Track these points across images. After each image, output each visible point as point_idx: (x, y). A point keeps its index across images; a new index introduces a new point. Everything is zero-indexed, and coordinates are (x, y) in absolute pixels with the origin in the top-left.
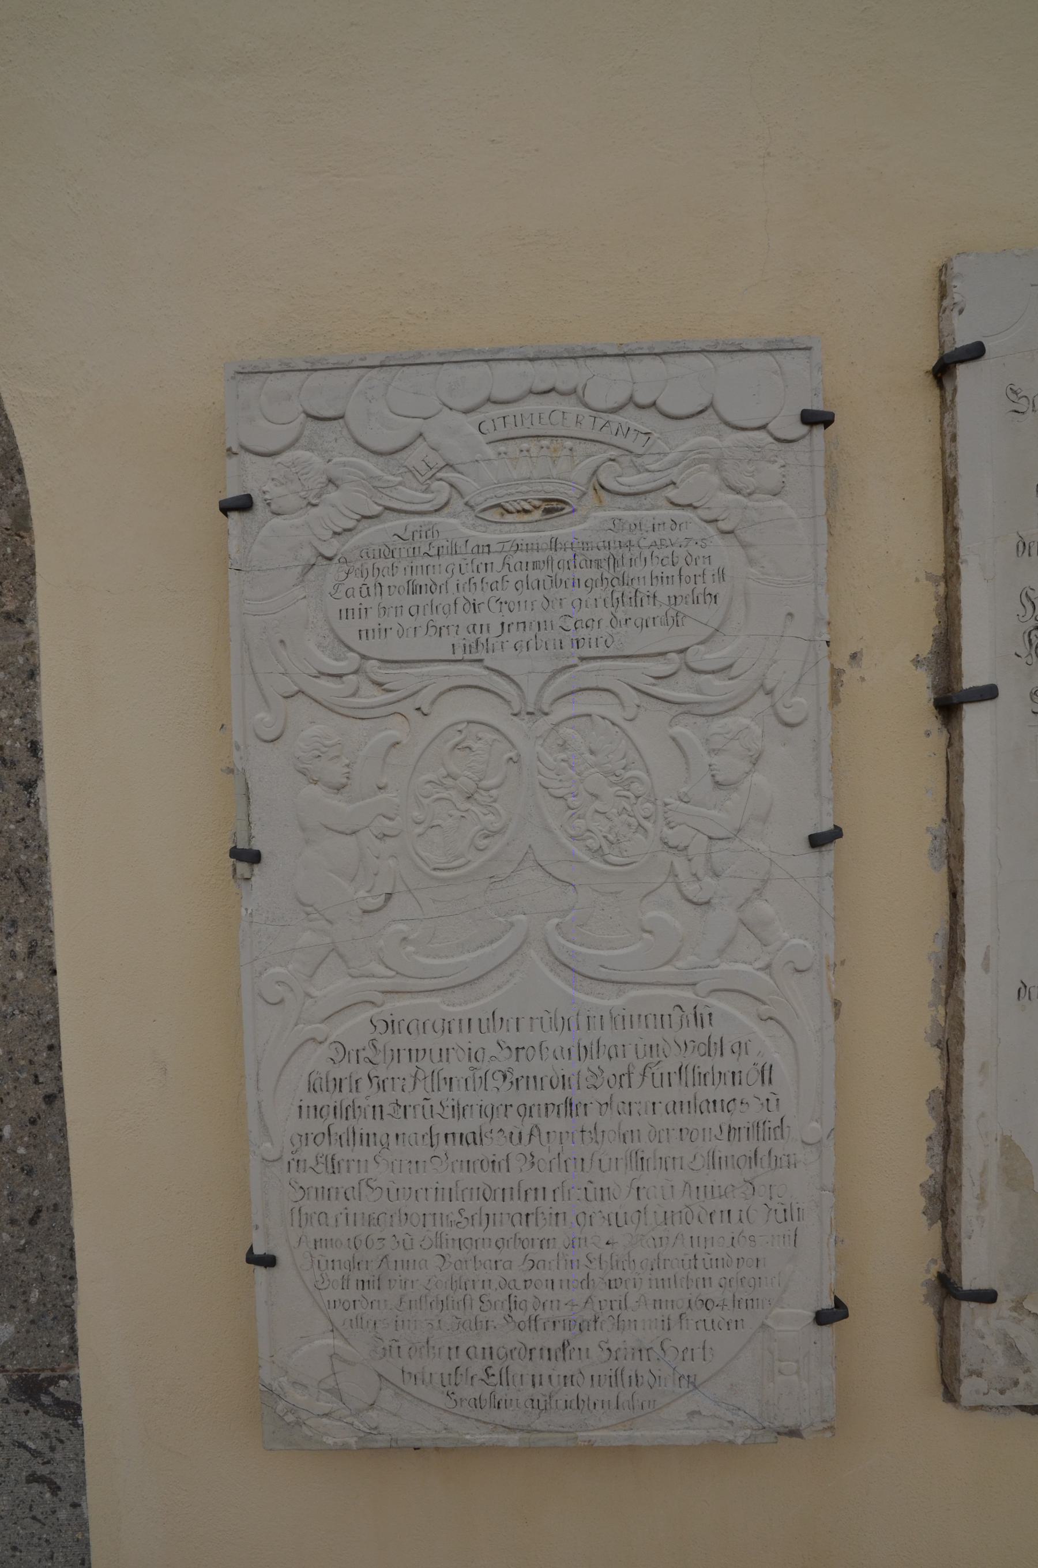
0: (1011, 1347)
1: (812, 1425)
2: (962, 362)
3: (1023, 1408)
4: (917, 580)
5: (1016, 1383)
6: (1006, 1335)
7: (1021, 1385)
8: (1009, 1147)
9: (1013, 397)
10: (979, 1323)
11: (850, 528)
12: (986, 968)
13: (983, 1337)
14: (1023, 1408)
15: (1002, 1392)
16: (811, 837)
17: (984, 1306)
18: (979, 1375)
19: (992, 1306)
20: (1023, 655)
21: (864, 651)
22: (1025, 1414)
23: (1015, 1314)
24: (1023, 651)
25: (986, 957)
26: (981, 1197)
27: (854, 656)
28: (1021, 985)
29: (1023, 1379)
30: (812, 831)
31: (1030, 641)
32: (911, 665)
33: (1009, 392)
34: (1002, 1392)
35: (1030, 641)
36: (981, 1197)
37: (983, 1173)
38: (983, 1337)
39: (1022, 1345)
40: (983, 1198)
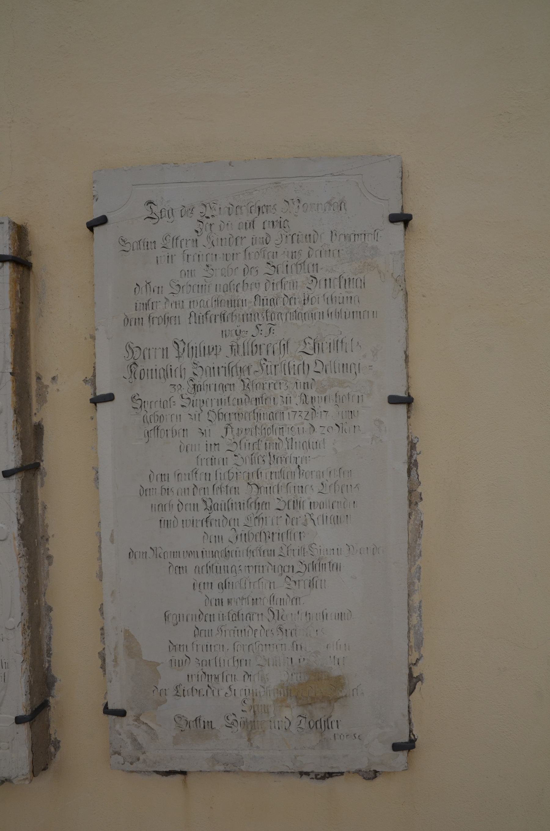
0: (134, 740)
1: (17, 776)
2: (96, 226)
3: (157, 772)
4: (86, 339)
5: (138, 759)
6: (132, 734)
7: (141, 760)
8: (128, 636)
9: (122, 243)
10: (118, 727)
11: (51, 313)
12: (112, 541)
13: (120, 734)
14: (157, 772)
15: (132, 763)
16: (3, 472)
17: (120, 718)
18: (119, 754)
19: (124, 719)
20: (128, 378)
21: (59, 376)
22: (158, 775)
23: (136, 723)
24: (127, 375)
25: (112, 536)
26: (115, 660)
27: (54, 378)
28: (130, 551)
29: (142, 757)
30: (4, 469)
31: (131, 370)
32: (83, 382)
33: (121, 241)
34: (132, 763)
35: (131, 370)
36: (115, 660)
37: (115, 649)
38: (120, 734)
39: (140, 739)
40: (116, 662)
